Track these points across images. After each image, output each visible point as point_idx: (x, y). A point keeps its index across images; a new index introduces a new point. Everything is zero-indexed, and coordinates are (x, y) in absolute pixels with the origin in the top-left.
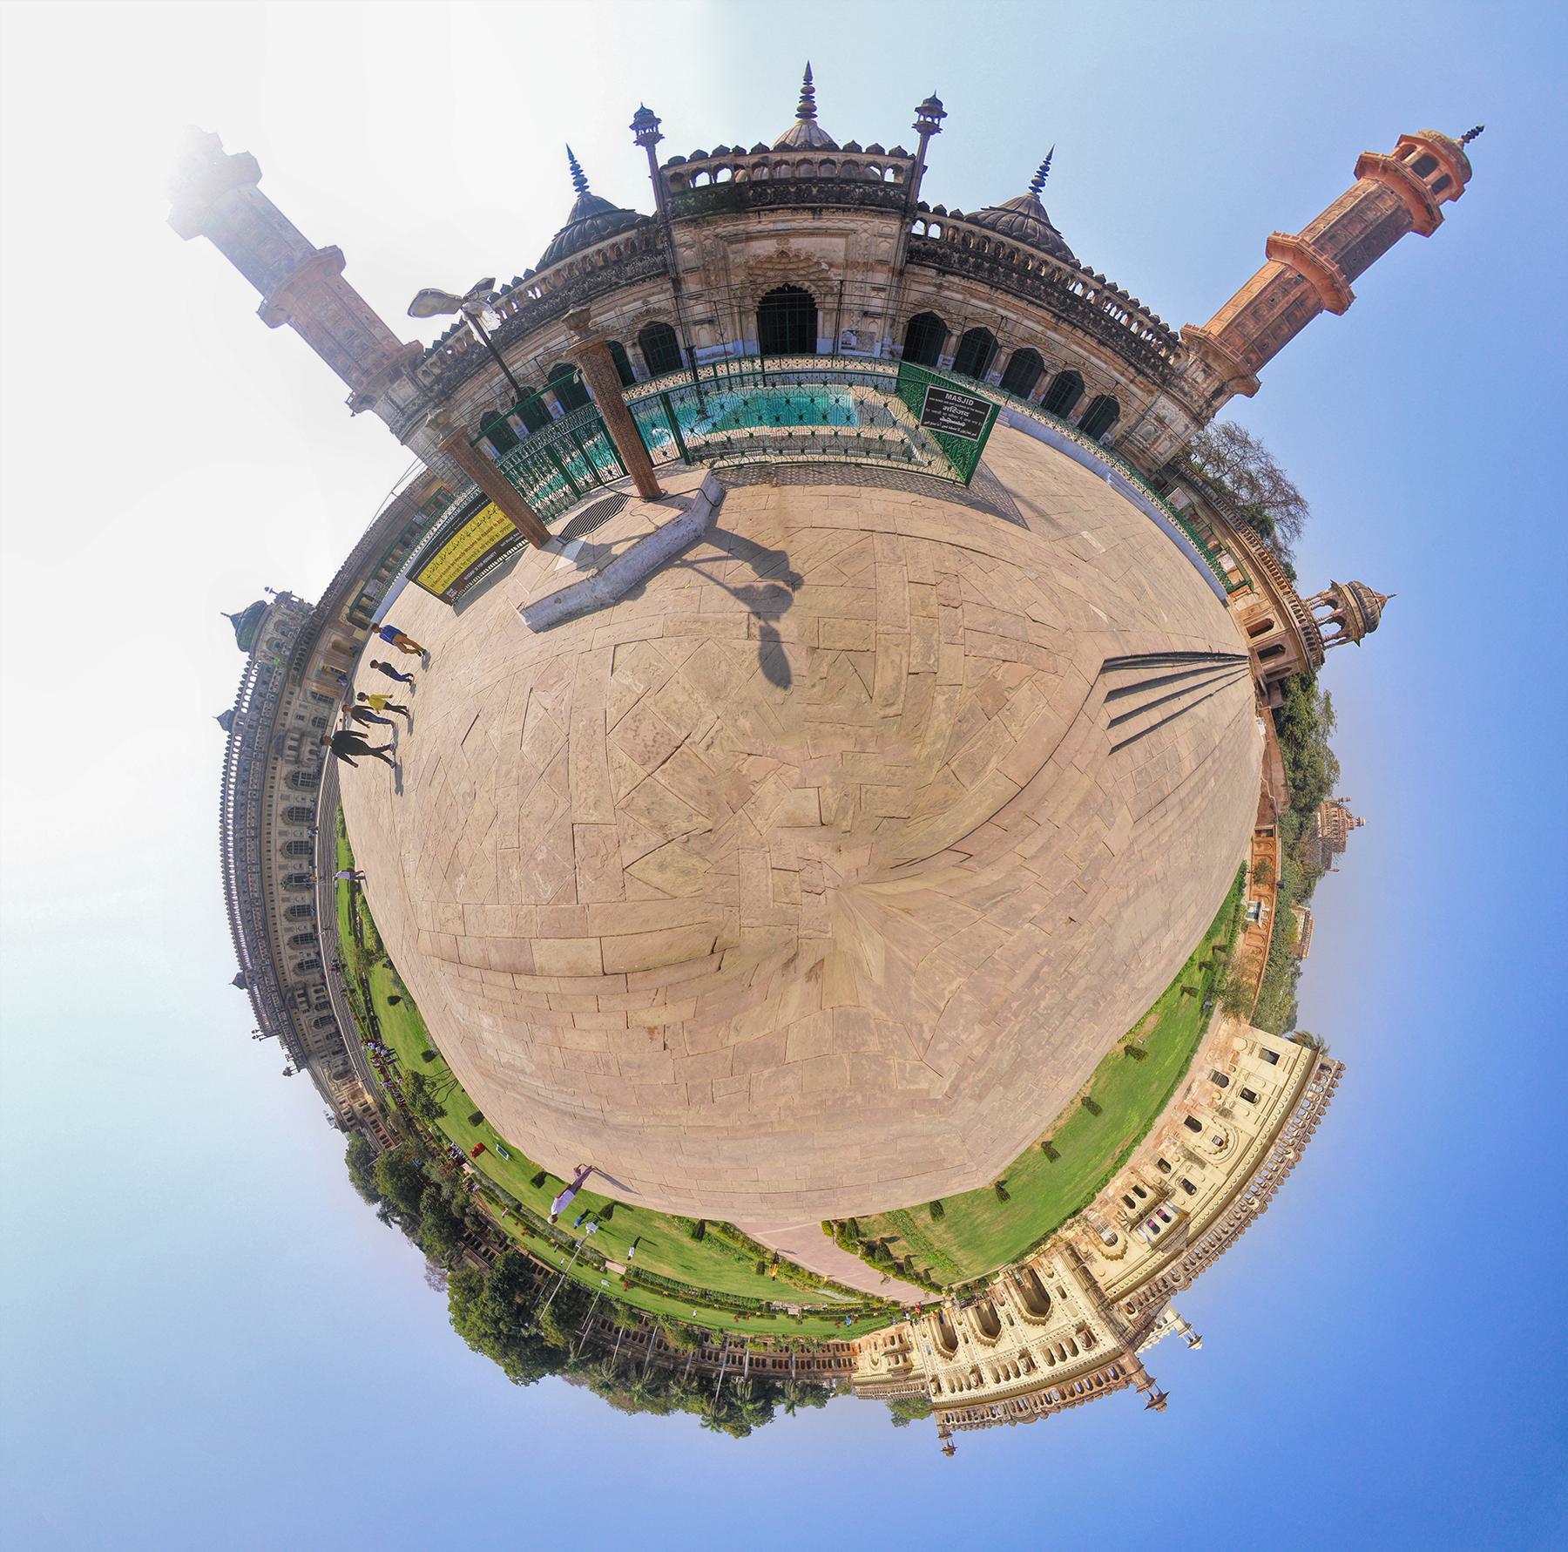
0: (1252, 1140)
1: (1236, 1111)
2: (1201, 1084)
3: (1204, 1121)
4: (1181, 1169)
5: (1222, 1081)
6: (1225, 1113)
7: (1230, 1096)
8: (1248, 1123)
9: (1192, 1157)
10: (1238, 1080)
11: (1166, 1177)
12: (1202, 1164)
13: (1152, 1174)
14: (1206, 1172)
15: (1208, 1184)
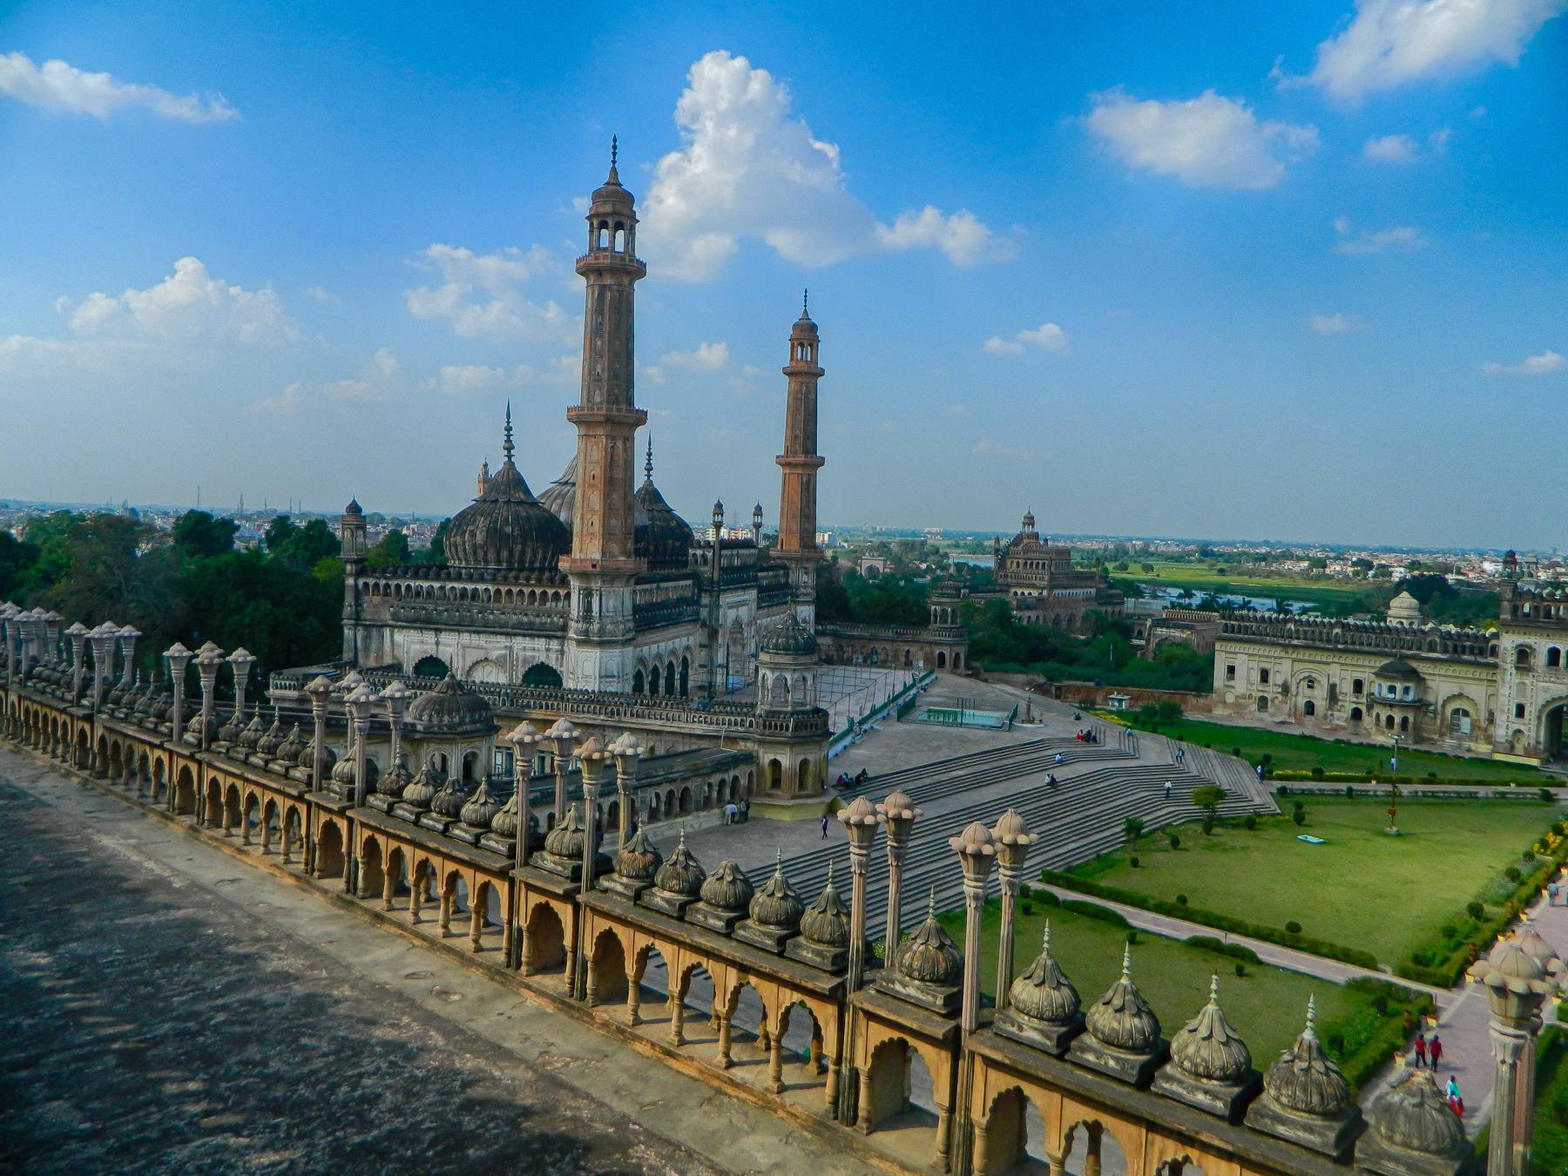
0: (1294, 660)
1: (1280, 682)
2: (1273, 715)
3: (1301, 702)
4: (1348, 703)
5: (1263, 703)
6: (1286, 689)
7: (1271, 691)
8: (1284, 668)
9: (1333, 697)
10: (1257, 690)
11: (1363, 708)
12: (1333, 687)
13: (1368, 721)
14: (1337, 681)
15: (1347, 675)
